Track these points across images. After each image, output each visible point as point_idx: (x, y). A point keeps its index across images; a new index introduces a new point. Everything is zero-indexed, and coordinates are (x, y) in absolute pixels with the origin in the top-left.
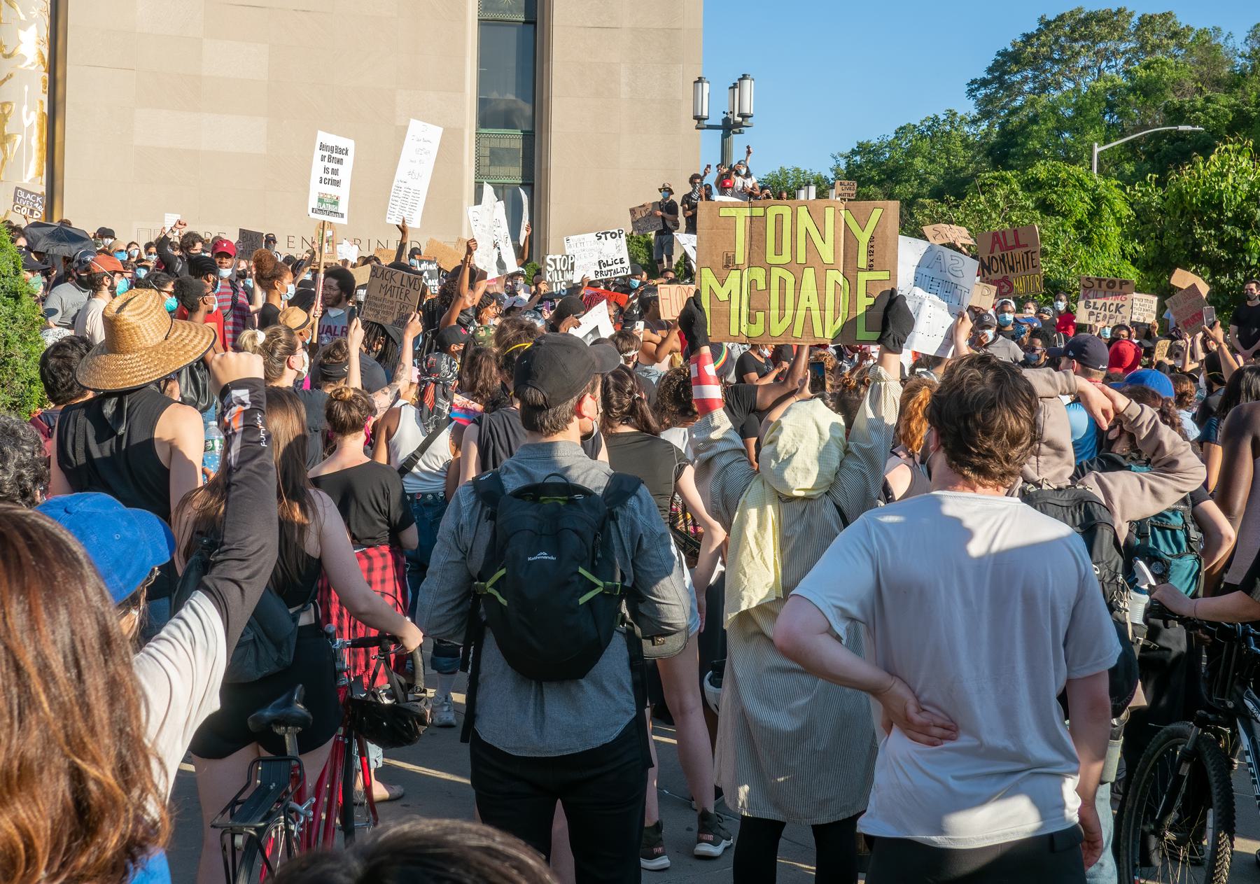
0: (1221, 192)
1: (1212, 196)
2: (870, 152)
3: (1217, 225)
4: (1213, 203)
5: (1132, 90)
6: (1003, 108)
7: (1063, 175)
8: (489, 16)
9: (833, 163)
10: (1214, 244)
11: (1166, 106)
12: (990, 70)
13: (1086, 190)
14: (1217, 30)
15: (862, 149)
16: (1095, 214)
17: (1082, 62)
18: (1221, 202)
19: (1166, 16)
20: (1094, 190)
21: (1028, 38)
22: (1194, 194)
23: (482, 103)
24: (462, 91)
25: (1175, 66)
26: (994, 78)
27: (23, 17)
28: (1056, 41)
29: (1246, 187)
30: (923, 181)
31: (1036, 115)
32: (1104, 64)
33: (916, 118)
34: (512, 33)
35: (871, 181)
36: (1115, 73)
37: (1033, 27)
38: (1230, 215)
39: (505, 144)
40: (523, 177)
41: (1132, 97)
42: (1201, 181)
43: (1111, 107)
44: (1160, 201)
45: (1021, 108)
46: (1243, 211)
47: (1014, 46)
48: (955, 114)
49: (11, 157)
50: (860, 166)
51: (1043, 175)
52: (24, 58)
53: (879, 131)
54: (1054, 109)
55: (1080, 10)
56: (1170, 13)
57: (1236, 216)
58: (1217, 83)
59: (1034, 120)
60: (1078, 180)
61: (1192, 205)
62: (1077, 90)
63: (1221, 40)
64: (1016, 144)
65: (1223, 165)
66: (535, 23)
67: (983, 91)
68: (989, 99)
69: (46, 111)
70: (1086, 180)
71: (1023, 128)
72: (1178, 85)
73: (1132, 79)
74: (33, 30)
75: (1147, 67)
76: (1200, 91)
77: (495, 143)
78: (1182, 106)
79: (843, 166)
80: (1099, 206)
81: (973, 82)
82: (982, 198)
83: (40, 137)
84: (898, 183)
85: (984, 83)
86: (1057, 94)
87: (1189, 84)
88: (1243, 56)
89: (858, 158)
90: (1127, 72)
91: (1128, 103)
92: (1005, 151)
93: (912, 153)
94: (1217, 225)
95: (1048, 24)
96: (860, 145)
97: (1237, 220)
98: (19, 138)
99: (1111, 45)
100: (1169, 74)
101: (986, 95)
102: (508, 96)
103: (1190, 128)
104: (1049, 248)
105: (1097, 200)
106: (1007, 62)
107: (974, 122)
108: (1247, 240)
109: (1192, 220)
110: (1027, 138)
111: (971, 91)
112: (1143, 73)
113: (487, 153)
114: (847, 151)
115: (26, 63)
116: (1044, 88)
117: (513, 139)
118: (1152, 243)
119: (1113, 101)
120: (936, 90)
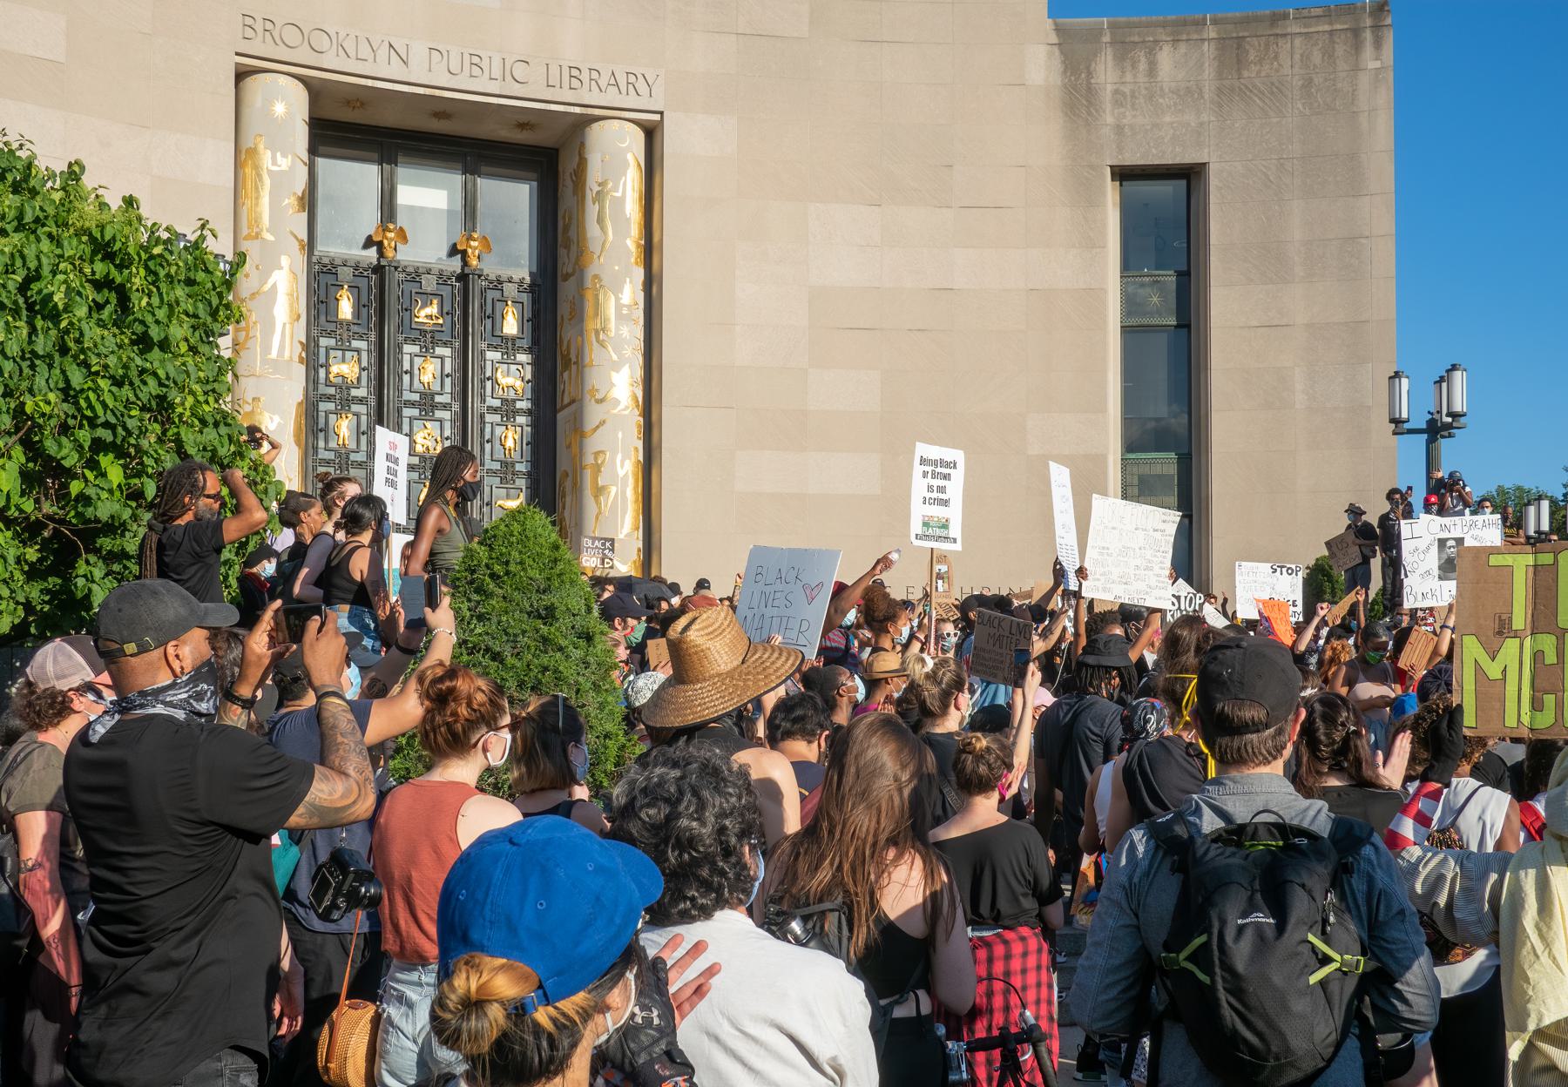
8: (1134, 321)
23: (1128, 421)
24: (1103, 410)
27: (615, 357)
34: (1162, 340)
39: (1157, 470)
49: (606, 510)
52: (617, 402)
66: (1188, 326)
69: (641, 458)
74: (626, 370)
77: (1145, 470)
83: (636, 487)
98: (613, 490)
102: (1160, 408)
113: (1136, 481)
115: (622, 406)
117: (1165, 463)
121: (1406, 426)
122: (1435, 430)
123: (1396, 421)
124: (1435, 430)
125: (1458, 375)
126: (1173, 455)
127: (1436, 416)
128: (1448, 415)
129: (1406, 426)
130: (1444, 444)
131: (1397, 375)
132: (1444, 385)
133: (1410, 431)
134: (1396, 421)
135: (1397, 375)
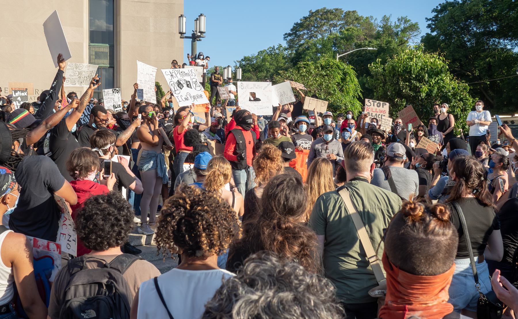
0: (411, 66)
1: (407, 68)
2: (248, 60)
3: (409, 81)
4: (408, 71)
5: (342, 38)
6: (296, 44)
7: (331, 64)
9: (234, 64)
10: (408, 89)
11: (355, 44)
12: (292, 30)
13: (341, 70)
14: (372, 17)
15: (245, 59)
16: (343, 80)
17: (325, 28)
18: (411, 71)
19: (354, 12)
20: (344, 70)
21: (305, 18)
22: (400, 67)
25: (358, 30)
26: (293, 33)
28: (316, 20)
29: (420, 64)
30: (268, 71)
31: (308, 47)
32: (332, 29)
33: (265, 46)
35: (249, 71)
36: (336, 32)
37: (307, 14)
38: (414, 76)
40: (110, 64)
41: (342, 41)
42: (402, 61)
43: (335, 45)
44: (382, 70)
45: (303, 44)
46: (420, 74)
47: (301, 20)
48: (281, 47)
50: (244, 66)
51: (323, 64)
53: (252, 52)
54: (315, 45)
55: (325, 8)
56: (355, 11)
57: (416, 76)
58: (371, 36)
59: (308, 49)
60: (337, 65)
61: (398, 71)
62: (323, 38)
63: (372, 21)
64: (302, 58)
65: (411, 54)
67: (289, 38)
68: (292, 41)
70: (340, 66)
71: (304, 51)
72: (358, 37)
73: (342, 35)
75: (347, 30)
76: (366, 39)
78: (361, 44)
79: (238, 66)
80: (345, 76)
81: (286, 34)
82: (305, 70)
84: (260, 72)
85: (290, 35)
86: (316, 39)
87: (362, 37)
88: (380, 27)
89: (244, 62)
90: (340, 32)
91: (341, 43)
92: (296, 60)
93: (264, 60)
94: (409, 81)
95: (313, 13)
96: (245, 58)
97: (415, 79)
99: (334, 22)
100: (356, 33)
101: (290, 39)
103: (372, 49)
104: (332, 92)
105: (345, 74)
106: (298, 27)
107: (286, 49)
108: (421, 87)
109: (398, 79)
110: (305, 55)
111: (285, 37)
112: (346, 32)
114: (240, 60)
116: (311, 37)
117: (105, 48)
118: (381, 89)
119: (335, 42)
120: (271, 37)
121: (185, 35)
122: (195, 38)
123: (181, 33)
124: (195, 38)
125: (202, 18)
126: (107, 45)
127: (195, 33)
128: (200, 32)
129: (185, 35)
130: (197, 43)
131: (182, 16)
132: (198, 21)
133: (186, 37)
134: (181, 33)
135: (182, 16)
